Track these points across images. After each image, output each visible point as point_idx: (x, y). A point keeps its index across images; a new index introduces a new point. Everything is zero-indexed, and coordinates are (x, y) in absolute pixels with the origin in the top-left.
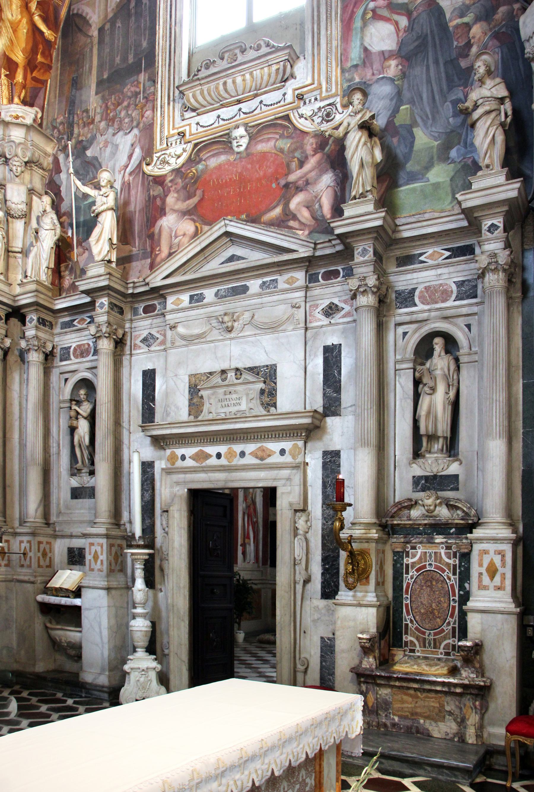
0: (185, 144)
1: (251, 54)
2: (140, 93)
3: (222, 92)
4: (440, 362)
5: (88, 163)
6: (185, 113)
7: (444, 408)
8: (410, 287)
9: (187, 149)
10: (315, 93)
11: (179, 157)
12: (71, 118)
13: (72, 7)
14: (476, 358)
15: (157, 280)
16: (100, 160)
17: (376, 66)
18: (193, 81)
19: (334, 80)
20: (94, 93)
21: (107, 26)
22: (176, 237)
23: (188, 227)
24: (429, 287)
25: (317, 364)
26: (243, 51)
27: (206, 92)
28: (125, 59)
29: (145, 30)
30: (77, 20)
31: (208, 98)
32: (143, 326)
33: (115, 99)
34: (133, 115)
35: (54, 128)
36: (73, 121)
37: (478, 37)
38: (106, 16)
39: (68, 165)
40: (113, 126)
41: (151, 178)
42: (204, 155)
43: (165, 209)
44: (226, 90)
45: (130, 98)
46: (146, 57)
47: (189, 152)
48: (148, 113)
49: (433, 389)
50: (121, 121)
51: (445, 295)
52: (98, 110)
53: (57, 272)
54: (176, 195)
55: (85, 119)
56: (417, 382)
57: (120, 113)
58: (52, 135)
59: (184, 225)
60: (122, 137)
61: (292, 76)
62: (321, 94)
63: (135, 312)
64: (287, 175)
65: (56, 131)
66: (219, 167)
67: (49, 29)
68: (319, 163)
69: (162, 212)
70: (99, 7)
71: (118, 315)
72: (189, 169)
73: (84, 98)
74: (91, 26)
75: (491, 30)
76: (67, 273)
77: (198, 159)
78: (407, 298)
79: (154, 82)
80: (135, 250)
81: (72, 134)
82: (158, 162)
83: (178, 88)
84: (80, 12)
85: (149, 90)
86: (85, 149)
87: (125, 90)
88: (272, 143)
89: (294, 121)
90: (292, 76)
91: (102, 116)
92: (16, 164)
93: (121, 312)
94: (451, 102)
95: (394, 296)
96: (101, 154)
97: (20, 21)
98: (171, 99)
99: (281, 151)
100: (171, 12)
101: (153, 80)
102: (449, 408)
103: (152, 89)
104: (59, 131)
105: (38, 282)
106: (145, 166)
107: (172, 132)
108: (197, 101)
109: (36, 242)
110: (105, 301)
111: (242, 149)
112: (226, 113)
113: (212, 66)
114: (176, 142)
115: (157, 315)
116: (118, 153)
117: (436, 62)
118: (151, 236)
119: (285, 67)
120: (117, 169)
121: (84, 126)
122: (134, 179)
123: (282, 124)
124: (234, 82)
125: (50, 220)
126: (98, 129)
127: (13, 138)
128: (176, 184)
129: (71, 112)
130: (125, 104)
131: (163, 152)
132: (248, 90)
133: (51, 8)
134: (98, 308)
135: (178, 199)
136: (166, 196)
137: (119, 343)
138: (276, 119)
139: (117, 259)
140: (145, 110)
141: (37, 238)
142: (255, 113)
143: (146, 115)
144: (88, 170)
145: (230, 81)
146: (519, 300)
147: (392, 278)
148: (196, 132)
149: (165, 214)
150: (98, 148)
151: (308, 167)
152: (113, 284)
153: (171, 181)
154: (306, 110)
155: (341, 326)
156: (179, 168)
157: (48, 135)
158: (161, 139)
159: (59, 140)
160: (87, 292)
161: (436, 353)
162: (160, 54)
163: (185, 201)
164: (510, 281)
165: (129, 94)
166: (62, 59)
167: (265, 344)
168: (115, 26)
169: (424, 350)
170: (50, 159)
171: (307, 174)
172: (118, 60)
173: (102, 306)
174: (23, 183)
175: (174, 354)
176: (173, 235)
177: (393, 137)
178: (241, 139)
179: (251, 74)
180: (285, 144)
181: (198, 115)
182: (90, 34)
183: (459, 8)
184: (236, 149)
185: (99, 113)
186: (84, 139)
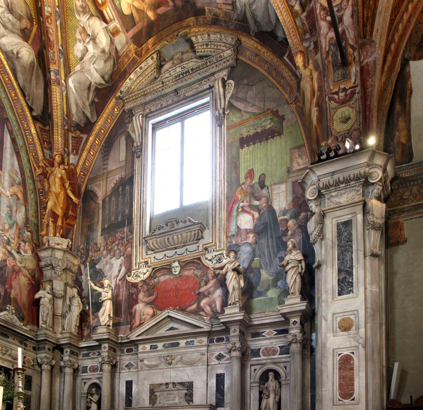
1: (181, 225)
3: (167, 243)
4: (272, 384)
5: (97, 272)
7: (274, 405)
8: (258, 348)
10: (213, 247)
11: (145, 274)
14: (289, 382)
15: (133, 337)
17: (243, 236)
19: (223, 242)
21: (107, 199)
22: (143, 315)
23: (149, 311)
24: (267, 348)
25: (213, 382)
26: (177, 223)
27: (158, 242)
28: (116, 218)
31: (160, 245)
32: (126, 359)
37: (291, 226)
38: (106, 194)
39: (87, 272)
42: (158, 274)
44: (169, 242)
45: (119, 240)
46: (128, 218)
48: (129, 249)
49: (268, 396)
50: (115, 252)
51: (274, 352)
52: (102, 244)
53: (80, 328)
56: (261, 393)
58: (77, 255)
61: (202, 238)
62: (216, 248)
63: (122, 351)
64: (199, 288)
66: (165, 281)
68: (215, 284)
70: (103, 188)
73: (94, 236)
75: (297, 224)
76: (86, 328)
78: (256, 353)
80: (122, 320)
81: (88, 256)
83: (144, 238)
86: (95, 264)
87: (117, 235)
88: (192, 272)
89: (203, 261)
90: (202, 238)
91: (104, 248)
92: (59, 270)
93: (115, 351)
94: (279, 258)
95: (250, 352)
99: (197, 276)
102: (276, 406)
104: (81, 253)
105: (71, 333)
107: (141, 261)
108: (154, 246)
111: (177, 273)
112: (169, 253)
113: (161, 230)
115: (134, 354)
117: (272, 237)
118: (131, 314)
119: (198, 233)
120: (113, 277)
121: (95, 252)
123: (197, 262)
124: (173, 238)
125: (77, 301)
126: (102, 254)
127: (57, 256)
129: (88, 244)
130: (117, 242)
132: (180, 243)
135: (144, 296)
136: (139, 294)
137: (114, 367)
138: (194, 259)
139: (113, 324)
141: (70, 310)
142: (184, 255)
143: (128, 250)
144: (98, 276)
145: (171, 238)
146: (309, 356)
147: (249, 343)
149: (138, 303)
151: (209, 285)
152: (110, 338)
153: (141, 286)
154: (209, 256)
155: (225, 365)
157: (75, 254)
159: (81, 258)
161: (270, 379)
163: (148, 297)
164: (304, 347)
165: (119, 238)
167: (187, 371)
169: (264, 378)
170: (76, 267)
171: (209, 288)
172: (113, 218)
175: (142, 374)
177: (251, 273)
178: (176, 269)
179: (181, 235)
180: (199, 273)
181: (155, 253)
183: (283, 211)
184: (174, 273)
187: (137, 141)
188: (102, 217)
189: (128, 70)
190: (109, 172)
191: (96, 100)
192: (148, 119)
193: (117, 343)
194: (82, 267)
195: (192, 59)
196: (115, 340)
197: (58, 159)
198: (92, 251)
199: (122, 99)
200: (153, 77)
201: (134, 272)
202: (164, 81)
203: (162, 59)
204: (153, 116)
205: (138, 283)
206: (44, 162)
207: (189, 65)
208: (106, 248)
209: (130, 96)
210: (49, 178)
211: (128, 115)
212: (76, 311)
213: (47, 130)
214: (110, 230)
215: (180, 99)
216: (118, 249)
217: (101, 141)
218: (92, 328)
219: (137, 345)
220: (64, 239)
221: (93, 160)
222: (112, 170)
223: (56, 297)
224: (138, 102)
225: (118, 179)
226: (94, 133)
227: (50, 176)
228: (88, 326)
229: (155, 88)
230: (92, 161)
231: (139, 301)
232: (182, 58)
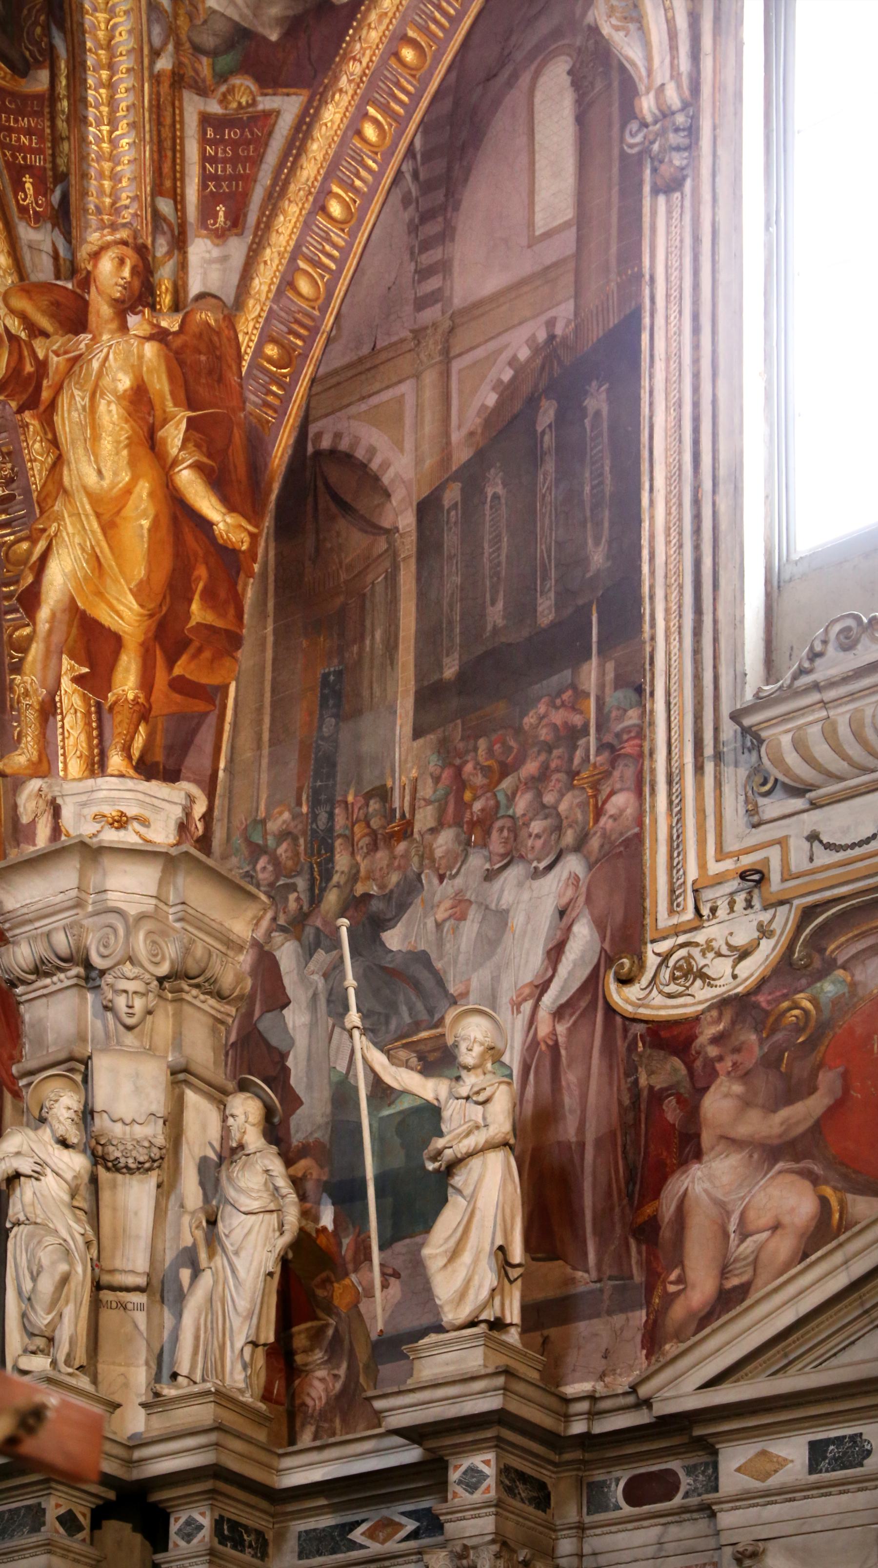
0: (765, 908)
2: (584, 731)
6: (761, 801)
9: (776, 926)
11: (744, 954)
12: (323, 817)
13: (313, 429)
16: (438, 965)
18: (792, 693)
20: (408, 730)
21: (452, 495)
22: (744, 1236)
28: (522, 609)
29: (596, 506)
30: (334, 474)
33: (490, 751)
34: (563, 807)
35: (256, 851)
36: (330, 829)
40: (485, 845)
41: (639, 1029)
42: (841, 947)
43: (698, 1136)
47: (784, 940)
48: (621, 801)
50: (515, 829)
52: (427, 790)
54: (738, 1088)
55: (375, 823)
57: (511, 799)
58: (249, 876)
59: (775, 1191)
60: (520, 885)
63: (596, 1498)
65: (262, 862)
67: (229, 504)
69: (687, 1146)
70: (418, 423)
71: (531, 1509)
72: (785, 997)
73: (368, 747)
74: (387, 495)
77: (817, 963)
79: (639, 690)
81: (327, 874)
82: (665, 974)
84: (344, 445)
85: (620, 719)
87: (529, 720)
91: (441, 812)
96: (440, 943)
98: (709, 750)
103: (632, 717)
104: (275, 861)
106: (612, 986)
107: (714, 868)
109: (211, 1256)
110: (485, 1462)
114: (732, 904)
115: (684, 1510)
116: (507, 938)
118: (647, 1232)
120: (506, 995)
121: (374, 847)
122: (571, 1031)
126: (426, 855)
128: (737, 1050)
129: (323, 799)
130: (531, 767)
131: (682, 939)
133: (238, 437)
134: (459, 1490)
135: (746, 1103)
140: (606, 790)
148: (806, 866)
149: (698, 1155)
150: (430, 924)
153: (716, 1040)
156: (748, 994)
157: (235, 876)
158: (672, 891)
159: (278, 894)
160: (413, 1434)
162: (660, 593)
163: (773, 1107)
166: (279, 608)
168: (482, 492)
170: (245, 960)
173: (473, 1478)
174: (150, 1051)
176: (732, 1227)
182: (386, 524)
185: (428, 802)
186: (374, 890)
190: (460, 319)
193: (553, 1440)
194: (287, 954)
196: (546, 1421)
197: (111, 273)
198: (350, 840)
201: (663, 946)
205: (696, 1019)
208: (454, 810)
212: (254, 1246)
214: (476, 689)
216: (541, 809)
217: (402, 123)
218: (363, 1355)
219: (709, 1448)
220: (157, 788)
221: (345, 252)
225: (524, 354)
228: (337, 1337)
230: (341, 263)
231: (707, 1139)
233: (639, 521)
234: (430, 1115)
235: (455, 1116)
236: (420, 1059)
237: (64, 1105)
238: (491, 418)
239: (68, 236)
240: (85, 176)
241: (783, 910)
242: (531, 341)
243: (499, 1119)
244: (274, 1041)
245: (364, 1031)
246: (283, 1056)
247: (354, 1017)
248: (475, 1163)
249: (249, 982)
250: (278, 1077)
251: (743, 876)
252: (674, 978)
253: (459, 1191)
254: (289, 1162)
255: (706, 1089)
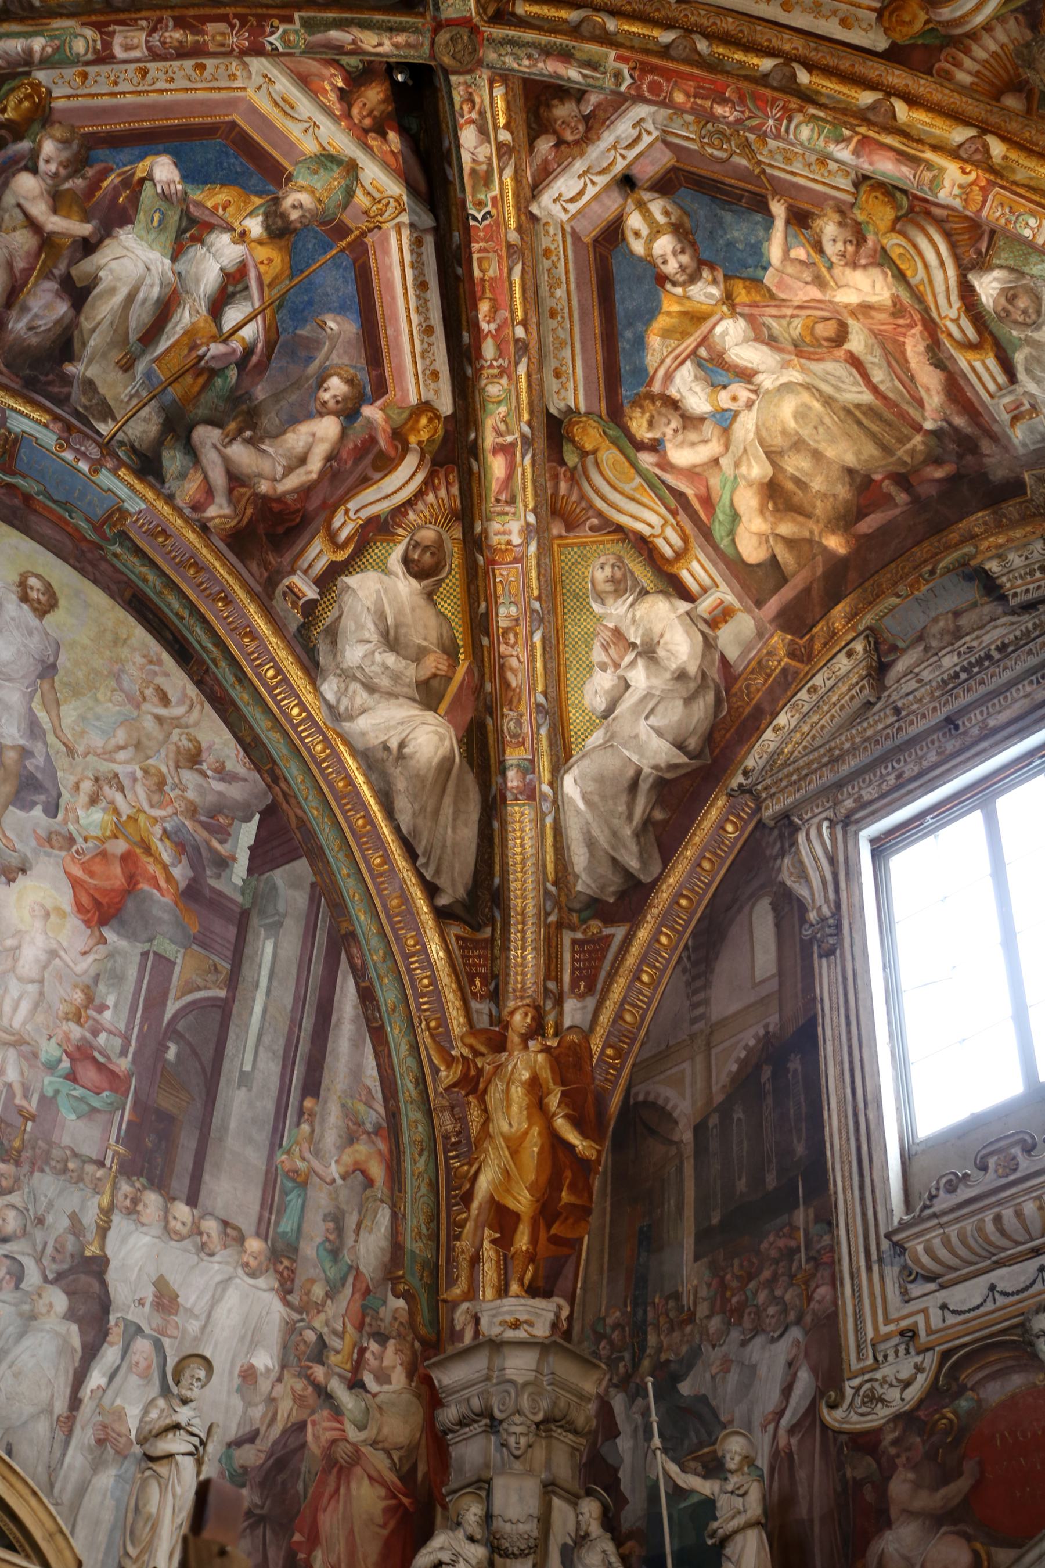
2: (798, 1250)
16: (714, 1403)
34: (787, 1297)
45: (777, 1262)
48: (823, 1292)
50: (759, 1312)
60: (763, 1348)
79: (830, 1223)
97: (526, 1133)
100: (853, 1082)
101: (826, 1219)
103: (826, 1240)
120: (757, 1419)
131: (867, 1377)
140: (813, 1285)
143: (817, 1296)
158: (858, 1346)
162: (838, 1167)
187: (820, 900)
188: (697, 1186)
189: (766, 706)
191: (658, 815)
192: (852, 828)
195: (993, 620)
199: (750, 792)
200: (857, 703)
202: (899, 704)
203: (884, 647)
204: (873, 813)
206: (470, 1040)
207: (987, 639)
208: (721, 1304)
209: (780, 775)
210: (485, 1091)
211: (776, 832)
213: (485, 940)
215: (968, 740)
216: (774, 1299)
222: (726, 1019)
223: (506, 1555)
224: (813, 786)
226: (653, 914)
227: (488, 1083)
229: (870, 732)
232: (958, 628)
233: (823, 1127)
234: (708, 1506)
235: (725, 1504)
236: (704, 1466)
237: (472, 1512)
238: (734, 1078)
239: (497, 1005)
240: (508, 975)
241: (929, 1354)
242: (756, 1036)
243: (753, 1506)
244: (610, 1461)
245: (665, 1451)
246: (616, 1470)
247: (657, 1441)
248: (739, 1538)
249: (594, 1423)
250: (612, 1486)
251: (902, 1334)
252: (864, 1403)
253: (729, 1559)
254: (619, 1543)
255: (890, 1478)
